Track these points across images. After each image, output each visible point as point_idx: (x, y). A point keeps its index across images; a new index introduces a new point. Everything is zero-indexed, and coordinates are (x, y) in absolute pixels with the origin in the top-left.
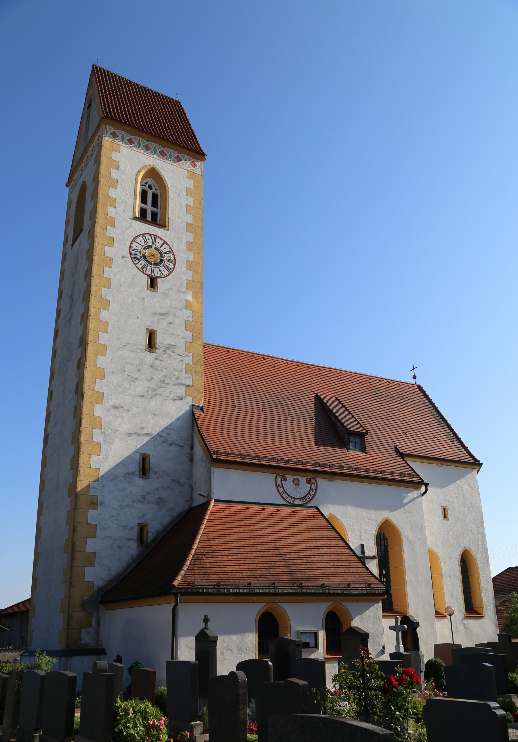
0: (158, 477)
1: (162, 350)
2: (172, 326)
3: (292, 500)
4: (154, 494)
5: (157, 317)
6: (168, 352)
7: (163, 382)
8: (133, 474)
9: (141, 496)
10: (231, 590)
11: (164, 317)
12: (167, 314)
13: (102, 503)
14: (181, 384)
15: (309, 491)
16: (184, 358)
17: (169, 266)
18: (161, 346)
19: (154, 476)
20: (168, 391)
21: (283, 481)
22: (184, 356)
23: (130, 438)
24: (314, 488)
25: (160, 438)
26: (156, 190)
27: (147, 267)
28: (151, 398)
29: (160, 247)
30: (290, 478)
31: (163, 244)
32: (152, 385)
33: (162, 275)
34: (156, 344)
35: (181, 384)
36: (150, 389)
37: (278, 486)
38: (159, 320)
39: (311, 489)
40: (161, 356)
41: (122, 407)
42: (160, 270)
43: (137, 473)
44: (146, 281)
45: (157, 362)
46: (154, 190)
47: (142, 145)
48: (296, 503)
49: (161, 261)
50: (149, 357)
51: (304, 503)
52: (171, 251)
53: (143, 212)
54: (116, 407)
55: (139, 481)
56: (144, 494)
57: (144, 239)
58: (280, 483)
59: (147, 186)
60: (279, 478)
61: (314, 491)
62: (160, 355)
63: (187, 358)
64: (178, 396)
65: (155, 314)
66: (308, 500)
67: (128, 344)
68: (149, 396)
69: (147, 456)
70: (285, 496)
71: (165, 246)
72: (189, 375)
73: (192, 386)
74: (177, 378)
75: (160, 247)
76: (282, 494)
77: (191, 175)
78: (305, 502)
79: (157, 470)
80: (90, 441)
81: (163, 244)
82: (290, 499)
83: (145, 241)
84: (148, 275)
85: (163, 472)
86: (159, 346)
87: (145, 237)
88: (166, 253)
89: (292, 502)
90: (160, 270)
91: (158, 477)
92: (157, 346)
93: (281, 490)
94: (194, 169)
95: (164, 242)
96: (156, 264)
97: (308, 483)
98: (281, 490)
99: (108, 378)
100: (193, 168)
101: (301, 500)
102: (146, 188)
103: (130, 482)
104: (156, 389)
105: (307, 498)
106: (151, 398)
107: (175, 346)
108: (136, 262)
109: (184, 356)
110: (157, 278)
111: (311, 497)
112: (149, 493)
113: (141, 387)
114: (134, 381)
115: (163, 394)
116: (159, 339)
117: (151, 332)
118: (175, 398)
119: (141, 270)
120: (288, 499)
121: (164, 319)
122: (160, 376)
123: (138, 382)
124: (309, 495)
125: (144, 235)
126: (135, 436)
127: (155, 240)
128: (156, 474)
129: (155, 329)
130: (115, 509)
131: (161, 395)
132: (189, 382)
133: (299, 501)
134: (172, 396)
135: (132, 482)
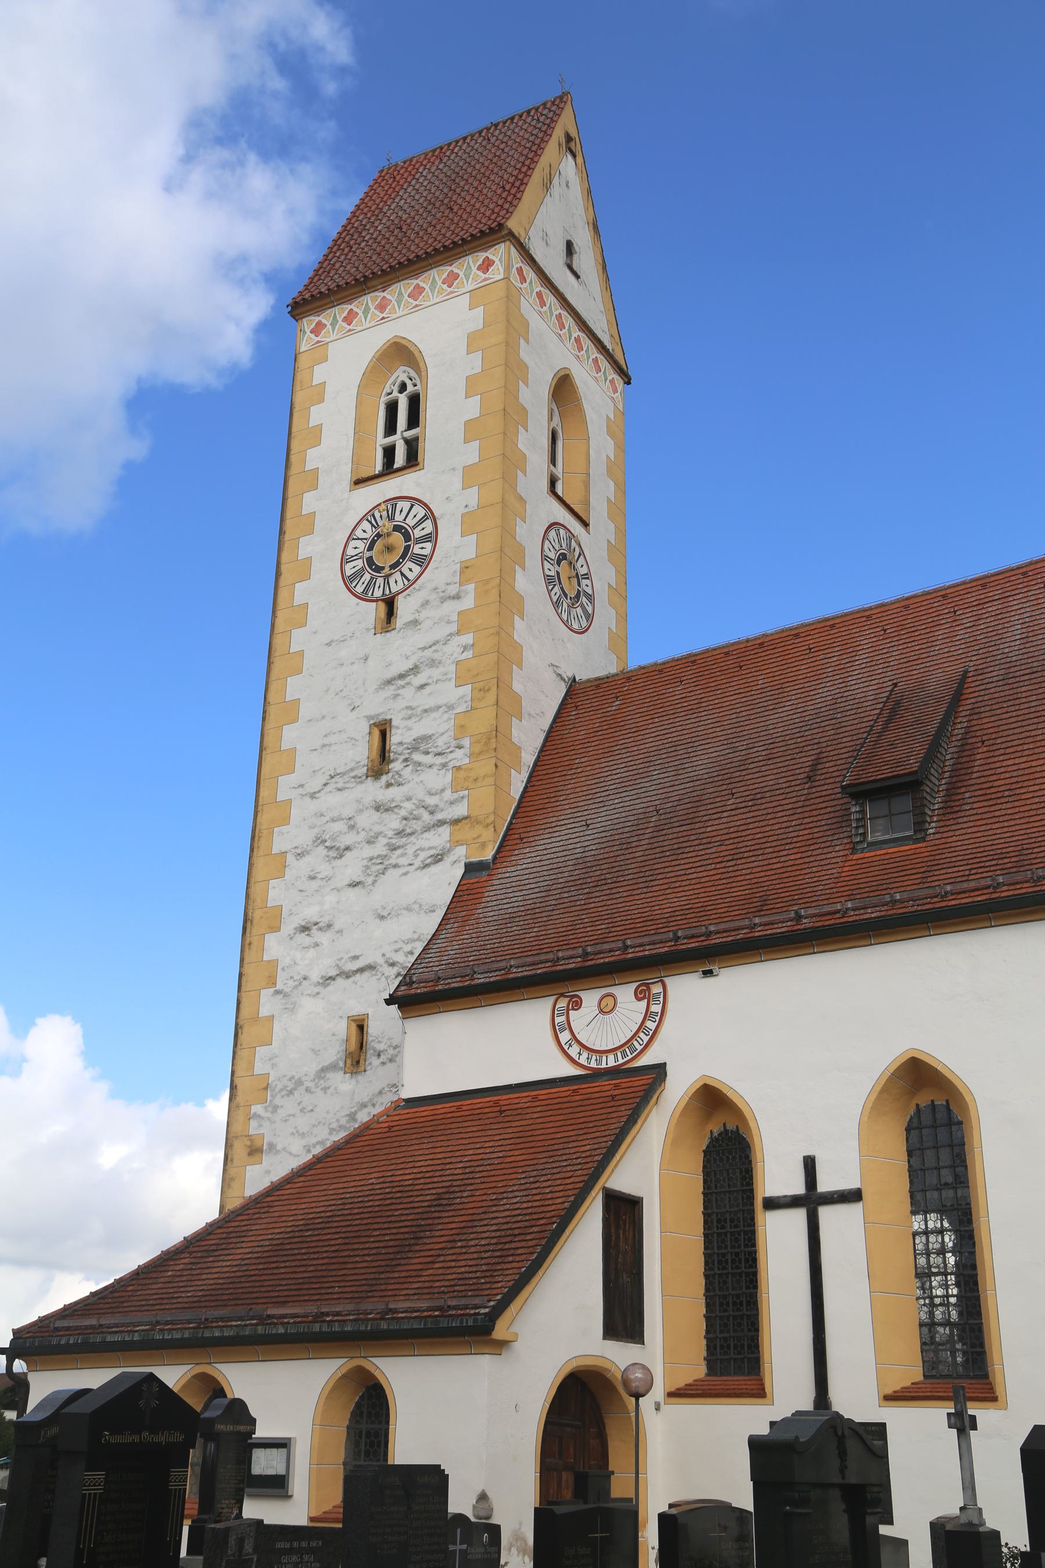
0: (383, 1063)
1: (402, 758)
2: (428, 690)
3: (594, 1058)
4: (374, 1105)
5: (391, 690)
6: (417, 757)
7: (400, 833)
8: (332, 1067)
9: (347, 1115)
10: (109, 1338)
11: (408, 679)
12: (415, 670)
13: (272, 1146)
14: (441, 823)
15: (643, 1022)
16: (451, 756)
18: (400, 749)
19: (375, 1062)
20: (410, 850)
21: (573, 1009)
22: (451, 752)
23: (330, 988)
24: (656, 1008)
25: (391, 968)
26: (415, 385)
27: (375, 583)
28: (375, 881)
29: (405, 520)
30: (590, 998)
31: (412, 506)
32: (380, 848)
33: (406, 582)
34: (389, 752)
35: (441, 823)
36: (373, 861)
37: (557, 1028)
38: (399, 692)
39: (648, 1014)
40: (400, 776)
41: (316, 924)
42: (402, 574)
43: (341, 1064)
44: (372, 612)
45: (394, 793)
46: (410, 388)
47: (372, 308)
48: (604, 1066)
49: (407, 549)
50: (374, 791)
51: (625, 1060)
52: (430, 515)
53: (389, 452)
54: (305, 929)
55: (343, 1083)
56: (353, 1110)
57: (370, 522)
58: (563, 1018)
59: (396, 389)
60: (563, 1003)
61: (657, 1018)
62: (397, 773)
63: (459, 753)
64: (432, 856)
65: (389, 682)
66: (639, 1048)
67: (332, 777)
68: (370, 880)
69: (363, 1020)
70: (574, 1051)
72: (461, 793)
73: (466, 818)
74: (432, 813)
75: (405, 520)
76: (566, 1047)
77: (476, 297)
78: (630, 1056)
79: (381, 1047)
80: (256, 1018)
81: (412, 506)
82: (588, 1058)
83: (373, 525)
84: (376, 601)
85: (395, 1048)
86: (395, 753)
87: (373, 515)
88: (414, 527)
89: (593, 1064)
90: (402, 574)
91: (383, 1063)
92: (392, 755)
93: (565, 1037)
94: (487, 276)
95: (414, 501)
97: (639, 999)
98: (565, 1037)
99: (297, 868)
100: (484, 276)
101: (594, 1058)
102: (395, 394)
103: (325, 1089)
104: (386, 856)
105: (635, 1043)
106: (374, 882)
107: (430, 737)
108: (354, 584)
109: (451, 752)
110: (394, 597)
111: (646, 1039)
112: (364, 1106)
113: (351, 867)
114: (341, 856)
115: (403, 861)
116: (395, 738)
117: (382, 728)
118: (429, 861)
119: (363, 597)
120: (583, 1060)
121: (408, 684)
122: (393, 822)
123: (348, 854)
124: (642, 1035)
125: (369, 516)
126: (340, 981)
128: (379, 1055)
129: (388, 717)
130: (295, 1156)
131: (396, 866)
132: (461, 810)
133: (611, 1057)
134: (418, 863)
135: (329, 1088)
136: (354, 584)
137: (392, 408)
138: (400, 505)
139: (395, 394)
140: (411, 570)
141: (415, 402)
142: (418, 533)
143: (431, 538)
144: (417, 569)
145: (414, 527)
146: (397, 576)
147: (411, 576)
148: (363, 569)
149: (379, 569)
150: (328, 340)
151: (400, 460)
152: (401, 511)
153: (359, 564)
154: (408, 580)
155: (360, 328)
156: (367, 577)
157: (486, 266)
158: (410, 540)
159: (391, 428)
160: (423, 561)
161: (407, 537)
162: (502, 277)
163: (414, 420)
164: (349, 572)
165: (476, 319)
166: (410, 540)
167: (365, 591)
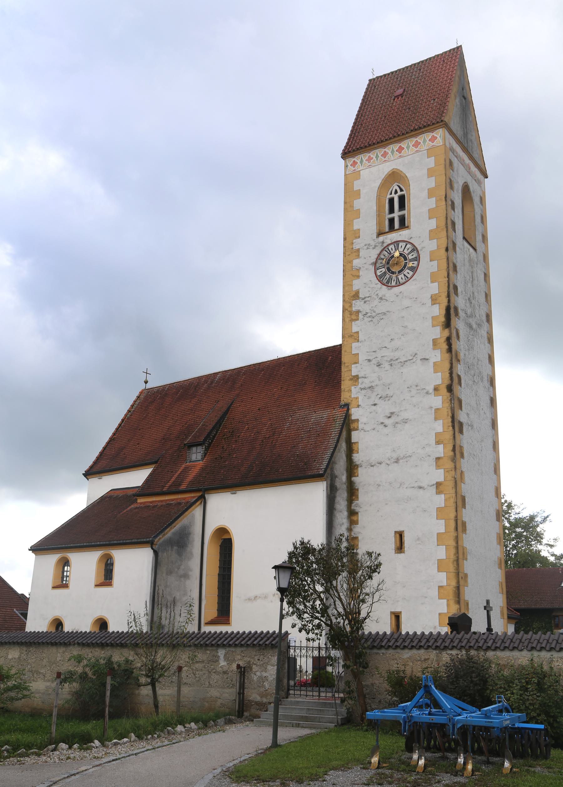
17: (413, 265)
42: (404, 275)
52: (415, 249)
53: (392, 221)
71: (408, 246)
77: (430, 152)
83: (388, 253)
87: (388, 249)
88: (408, 254)
90: (404, 275)
95: (407, 242)
96: (400, 272)
108: (382, 279)
127: (398, 245)
136: (382, 279)
137: (391, 201)
138: (401, 244)
139: (393, 195)
140: (408, 273)
141: (402, 199)
142: (410, 257)
143: (417, 259)
144: (411, 273)
145: (408, 254)
146: (402, 276)
147: (409, 276)
148: (385, 273)
149: (393, 273)
150: (359, 169)
151: (397, 225)
152: (401, 247)
153: (383, 270)
154: (407, 278)
155: (374, 165)
156: (388, 276)
157: (433, 139)
158: (407, 260)
159: (392, 210)
160: (414, 269)
161: (405, 259)
162: (441, 144)
163: (402, 206)
164: (379, 274)
165: (431, 162)
166: (407, 260)
167: (388, 282)
